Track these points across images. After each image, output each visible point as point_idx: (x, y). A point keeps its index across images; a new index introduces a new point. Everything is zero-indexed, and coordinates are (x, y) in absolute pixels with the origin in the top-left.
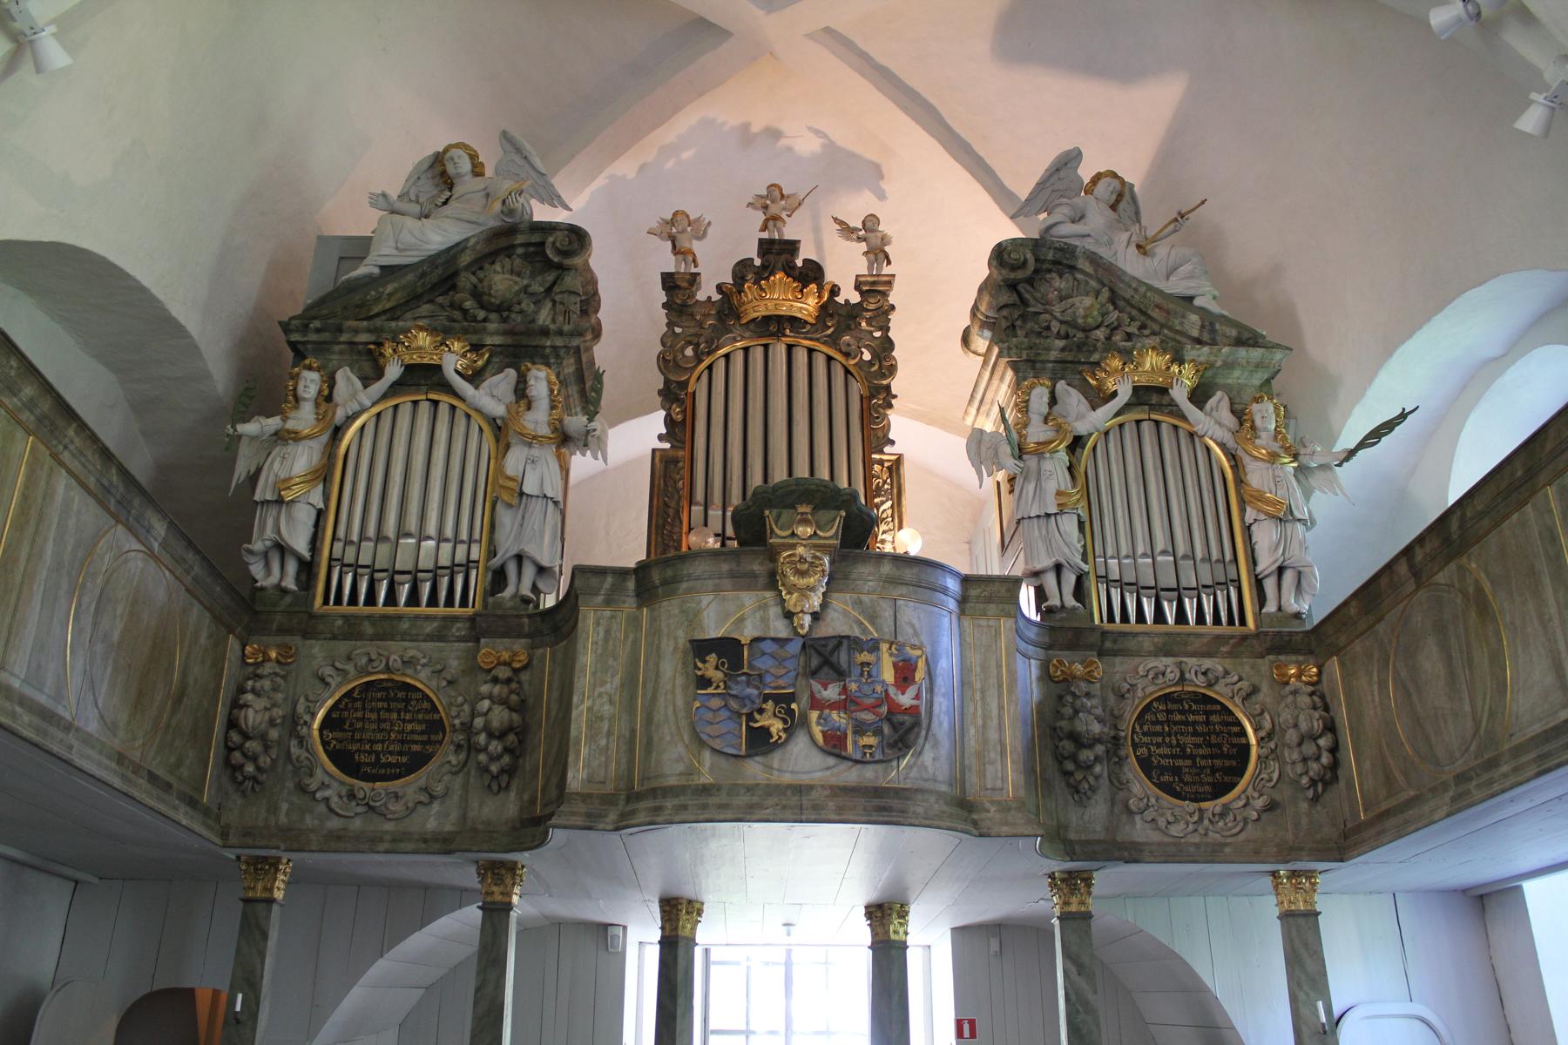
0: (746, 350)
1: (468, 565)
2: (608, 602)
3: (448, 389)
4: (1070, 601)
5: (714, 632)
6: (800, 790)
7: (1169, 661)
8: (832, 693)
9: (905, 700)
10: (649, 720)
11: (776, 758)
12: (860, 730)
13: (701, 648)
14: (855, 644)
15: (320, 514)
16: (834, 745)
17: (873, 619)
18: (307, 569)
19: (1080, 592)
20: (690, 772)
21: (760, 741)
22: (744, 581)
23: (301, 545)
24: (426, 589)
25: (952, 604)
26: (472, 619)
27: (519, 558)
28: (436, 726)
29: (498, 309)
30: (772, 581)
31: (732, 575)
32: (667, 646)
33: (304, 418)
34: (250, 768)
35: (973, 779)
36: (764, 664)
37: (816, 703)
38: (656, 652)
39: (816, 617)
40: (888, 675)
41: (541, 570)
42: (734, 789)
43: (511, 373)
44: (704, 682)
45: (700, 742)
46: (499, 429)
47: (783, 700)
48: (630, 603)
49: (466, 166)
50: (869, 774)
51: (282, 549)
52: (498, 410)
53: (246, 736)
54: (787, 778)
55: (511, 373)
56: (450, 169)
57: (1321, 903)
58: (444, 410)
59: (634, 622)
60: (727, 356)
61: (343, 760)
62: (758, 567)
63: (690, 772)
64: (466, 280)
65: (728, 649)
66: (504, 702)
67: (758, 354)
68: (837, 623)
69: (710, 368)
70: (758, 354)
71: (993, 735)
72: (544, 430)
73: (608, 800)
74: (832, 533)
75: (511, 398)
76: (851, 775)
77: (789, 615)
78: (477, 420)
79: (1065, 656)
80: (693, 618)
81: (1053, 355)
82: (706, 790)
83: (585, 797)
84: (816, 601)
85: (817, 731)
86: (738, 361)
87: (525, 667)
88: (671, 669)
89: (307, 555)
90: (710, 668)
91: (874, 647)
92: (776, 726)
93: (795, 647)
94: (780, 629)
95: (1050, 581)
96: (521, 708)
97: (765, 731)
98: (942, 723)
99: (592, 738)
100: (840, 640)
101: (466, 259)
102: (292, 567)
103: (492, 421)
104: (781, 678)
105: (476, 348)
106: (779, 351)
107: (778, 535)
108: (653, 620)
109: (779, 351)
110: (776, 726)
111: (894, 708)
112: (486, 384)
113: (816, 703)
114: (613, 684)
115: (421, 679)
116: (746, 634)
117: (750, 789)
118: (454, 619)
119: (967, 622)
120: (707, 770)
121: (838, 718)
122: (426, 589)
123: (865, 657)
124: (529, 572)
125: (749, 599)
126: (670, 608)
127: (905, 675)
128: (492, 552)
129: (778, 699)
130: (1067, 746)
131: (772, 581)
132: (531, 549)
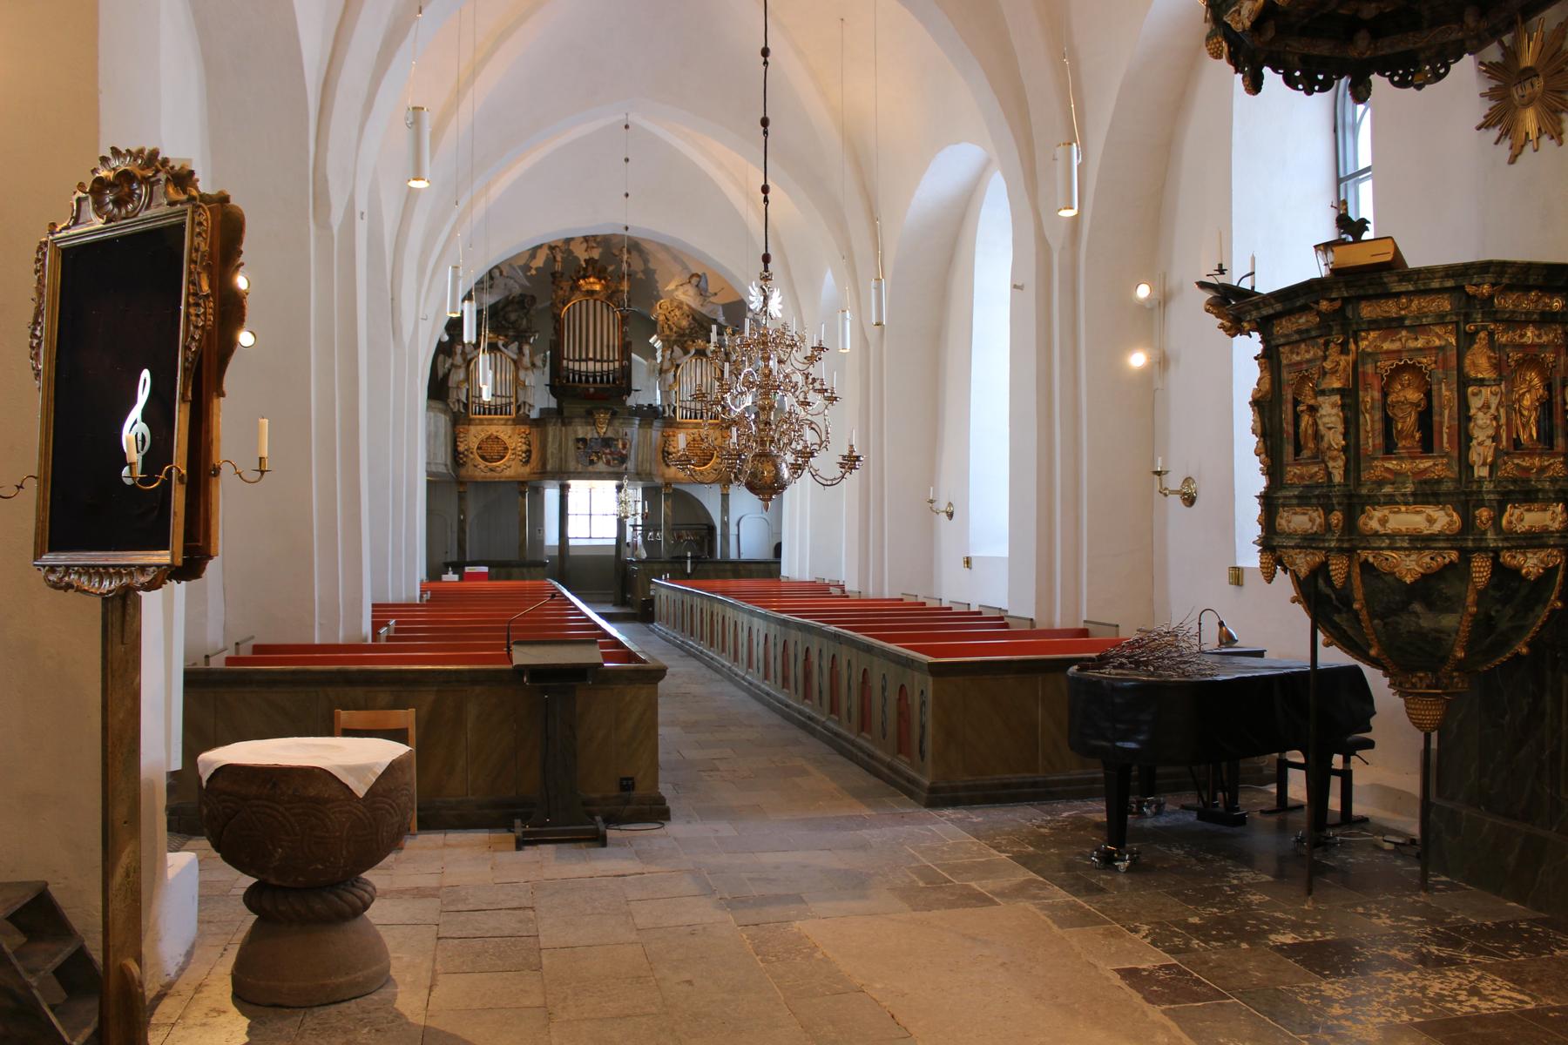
0: (580, 301)
1: (510, 403)
2: (554, 425)
3: (499, 350)
4: (672, 414)
5: (580, 436)
6: (600, 473)
7: (696, 430)
8: (608, 451)
9: (624, 452)
10: (566, 454)
11: (595, 466)
12: (614, 459)
13: (578, 440)
14: (614, 440)
15: (468, 390)
16: (608, 463)
17: (618, 432)
18: (466, 406)
19: (674, 411)
20: (576, 469)
21: (592, 462)
22: (588, 424)
23: (464, 399)
24: (499, 410)
25: (637, 426)
26: (514, 420)
27: (525, 403)
28: (506, 449)
29: (512, 323)
30: (594, 424)
31: (586, 422)
32: (570, 439)
33: (458, 359)
34: (461, 461)
35: (640, 468)
36: (592, 444)
37: (604, 453)
38: (567, 439)
39: (605, 433)
40: (620, 446)
41: (530, 405)
42: (586, 473)
43: (517, 343)
44: (579, 448)
45: (578, 462)
46: (515, 362)
47: (597, 453)
48: (559, 425)
49: (498, 274)
50: (616, 469)
51: (458, 401)
52: (515, 357)
53: (460, 453)
54: (597, 470)
55: (517, 343)
56: (493, 275)
57: (730, 491)
58: (498, 355)
59: (561, 430)
60: (574, 304)
61: (483, 458)
62: (592, 421)
63: (576, 469)
64: (502, 313)
65: (584, 440)
66: (525, 443)
67: (584, 302)
68: (610, 435)
69: (568, 309)
70: (584, 303)
71: (645, 457)
72: (529, 365)
73: (557, 473)
74: (608, 416)
75: (517, 351)
76: (611, 469)
77: (598, 433)
78: (508, 360)
79: (668, 429)
80: (576, 432)
81: (673, 338)
82: (580, 473)
83: (551, 472)
84: (605, 429)
85: (604, 460)
86: (578, 304)
87: (529, 434)
88: (571, 444)
89: (465, 401)
90: (580, 445)
91: (617, 440)
92: (595, 459)
93: (600, 440)
94: (596, 436)
95: (667, 408)
96: (529, 445)
97: (593, 460)
98: (632, 457)
99: (552, 458)
100: (610, 439)
101: (500, 305)
102: (461, 405)
103: (513, 360)
104: (596, 448)
105: (506, 336)
106: (591, 302)
107: (597, 416)
108: (566, 431)
109: (591, 302)
110: (595, 459)
111: (622, 454)
112: (509, 347)
113: (604, 453)
114: (557, 445)
115: (502, 436)
116: (589, 436)
117: (590, 473)
118: (508, 420)
119: (641, 430)
120: (580, 467)
121: (609, 457)
122: (499, 410)
123: (616, 442)
124: (527, 407)
125: (589, 428)
126: (570, 429)
127: (624, 446)
128: (517, 401)
129: (596, 452)
130: (666, 454)
131: (594, 424)
132: (527, 400)
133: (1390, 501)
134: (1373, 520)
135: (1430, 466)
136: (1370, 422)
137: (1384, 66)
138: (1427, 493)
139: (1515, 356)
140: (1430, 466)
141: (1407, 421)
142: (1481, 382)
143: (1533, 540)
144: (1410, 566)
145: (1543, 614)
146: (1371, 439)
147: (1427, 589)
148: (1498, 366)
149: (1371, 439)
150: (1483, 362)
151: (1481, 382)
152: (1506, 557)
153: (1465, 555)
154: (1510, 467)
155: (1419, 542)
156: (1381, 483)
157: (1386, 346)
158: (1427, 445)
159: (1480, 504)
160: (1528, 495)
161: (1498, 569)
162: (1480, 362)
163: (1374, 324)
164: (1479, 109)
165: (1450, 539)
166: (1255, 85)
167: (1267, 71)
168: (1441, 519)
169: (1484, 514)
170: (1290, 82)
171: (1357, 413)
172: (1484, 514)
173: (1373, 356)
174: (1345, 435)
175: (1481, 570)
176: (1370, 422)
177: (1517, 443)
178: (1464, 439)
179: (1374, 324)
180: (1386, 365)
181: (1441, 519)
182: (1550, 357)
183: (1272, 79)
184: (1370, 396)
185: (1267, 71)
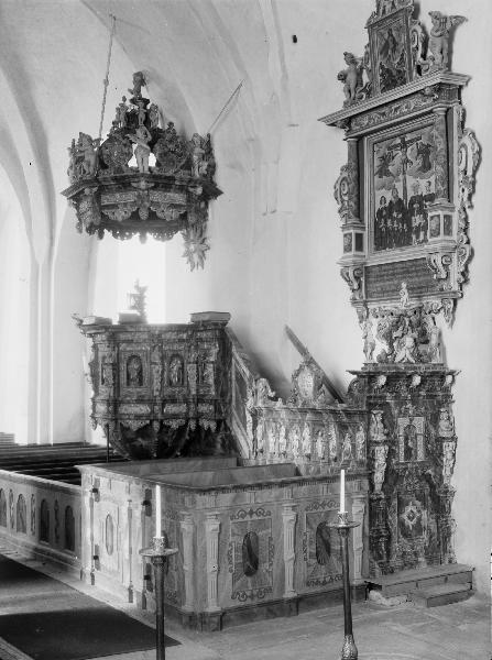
133: (129, 402)
134: (124, 409)
135: (142, 391)
136: (123, 375)
137: (153, 230)
138: (140, 401)
139: (170, 354)
140: (142, 391)
141: (134, 375)
142: (155, 364)
143: (175, 416)
144: (135, 425)
145: (183, 441)
146: (123, 380)
147: (144, 432)
148: (162, 358)
149: (123, 380)
150: (157, 357)
151: (155, 364)
152: (165, 423)
153: (151, 422)
154: (168, 391)
155: (138, 417)
156: (126, 396)
157: (128, 349)
158: (141, 383)
159: (155, 404)
160: (174, 401)
161: (162, 426)
162: (156, 357)
163: (124, 341)
164: (183, 249)
165: (148, 417)
166: (101, 236)
167: (105, 231)
168: (144, 409)
169: (157, 408)
170: (115, 235)
171: (119, 371)
172: (157, 408)
173: (125, 351)
174: (114, 379)
175: (156, 425)
176: (123, 375)
177: (170, 383)
178: (151, 382)
179: (124, 341)
180: (128, 355)
181: (144, 409)
182: (182, 353)
183: (108, 234)
184: (123, 366)
185: (105, 231)
